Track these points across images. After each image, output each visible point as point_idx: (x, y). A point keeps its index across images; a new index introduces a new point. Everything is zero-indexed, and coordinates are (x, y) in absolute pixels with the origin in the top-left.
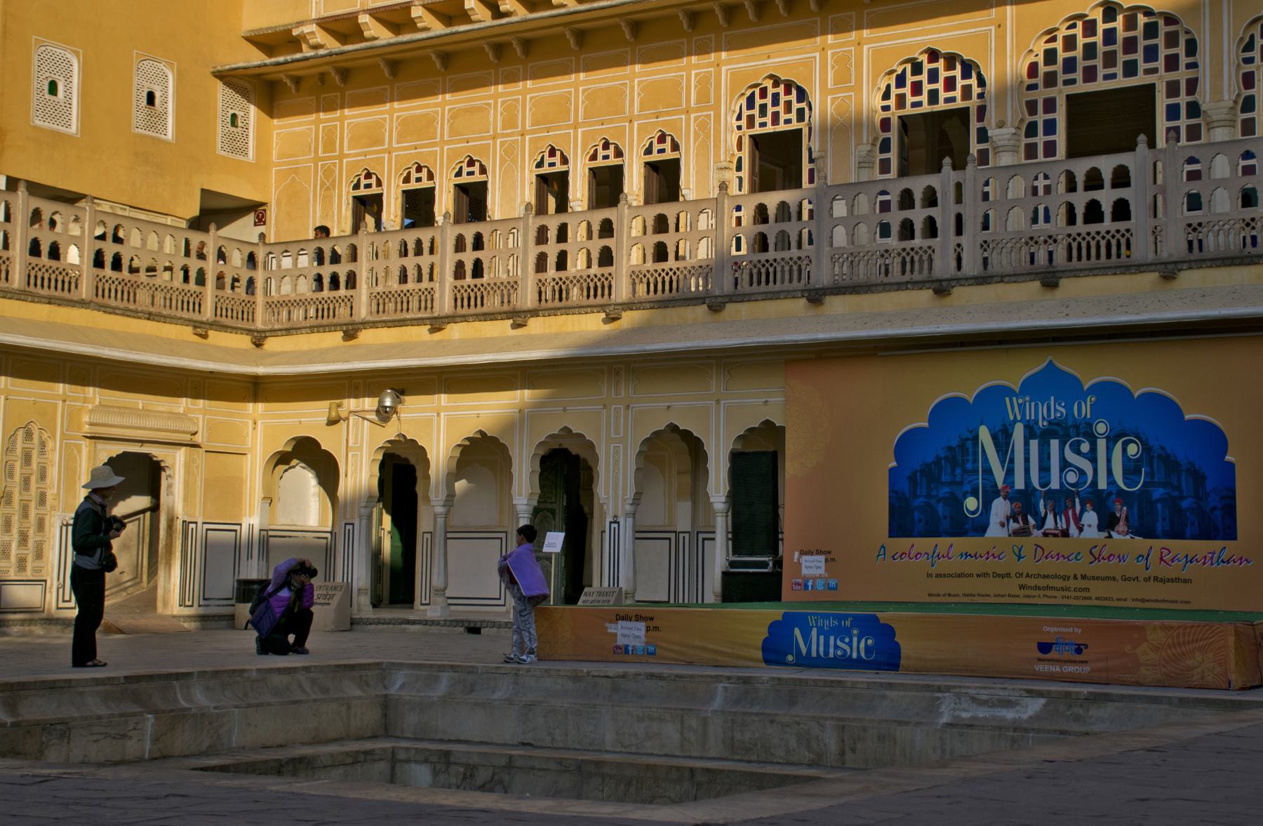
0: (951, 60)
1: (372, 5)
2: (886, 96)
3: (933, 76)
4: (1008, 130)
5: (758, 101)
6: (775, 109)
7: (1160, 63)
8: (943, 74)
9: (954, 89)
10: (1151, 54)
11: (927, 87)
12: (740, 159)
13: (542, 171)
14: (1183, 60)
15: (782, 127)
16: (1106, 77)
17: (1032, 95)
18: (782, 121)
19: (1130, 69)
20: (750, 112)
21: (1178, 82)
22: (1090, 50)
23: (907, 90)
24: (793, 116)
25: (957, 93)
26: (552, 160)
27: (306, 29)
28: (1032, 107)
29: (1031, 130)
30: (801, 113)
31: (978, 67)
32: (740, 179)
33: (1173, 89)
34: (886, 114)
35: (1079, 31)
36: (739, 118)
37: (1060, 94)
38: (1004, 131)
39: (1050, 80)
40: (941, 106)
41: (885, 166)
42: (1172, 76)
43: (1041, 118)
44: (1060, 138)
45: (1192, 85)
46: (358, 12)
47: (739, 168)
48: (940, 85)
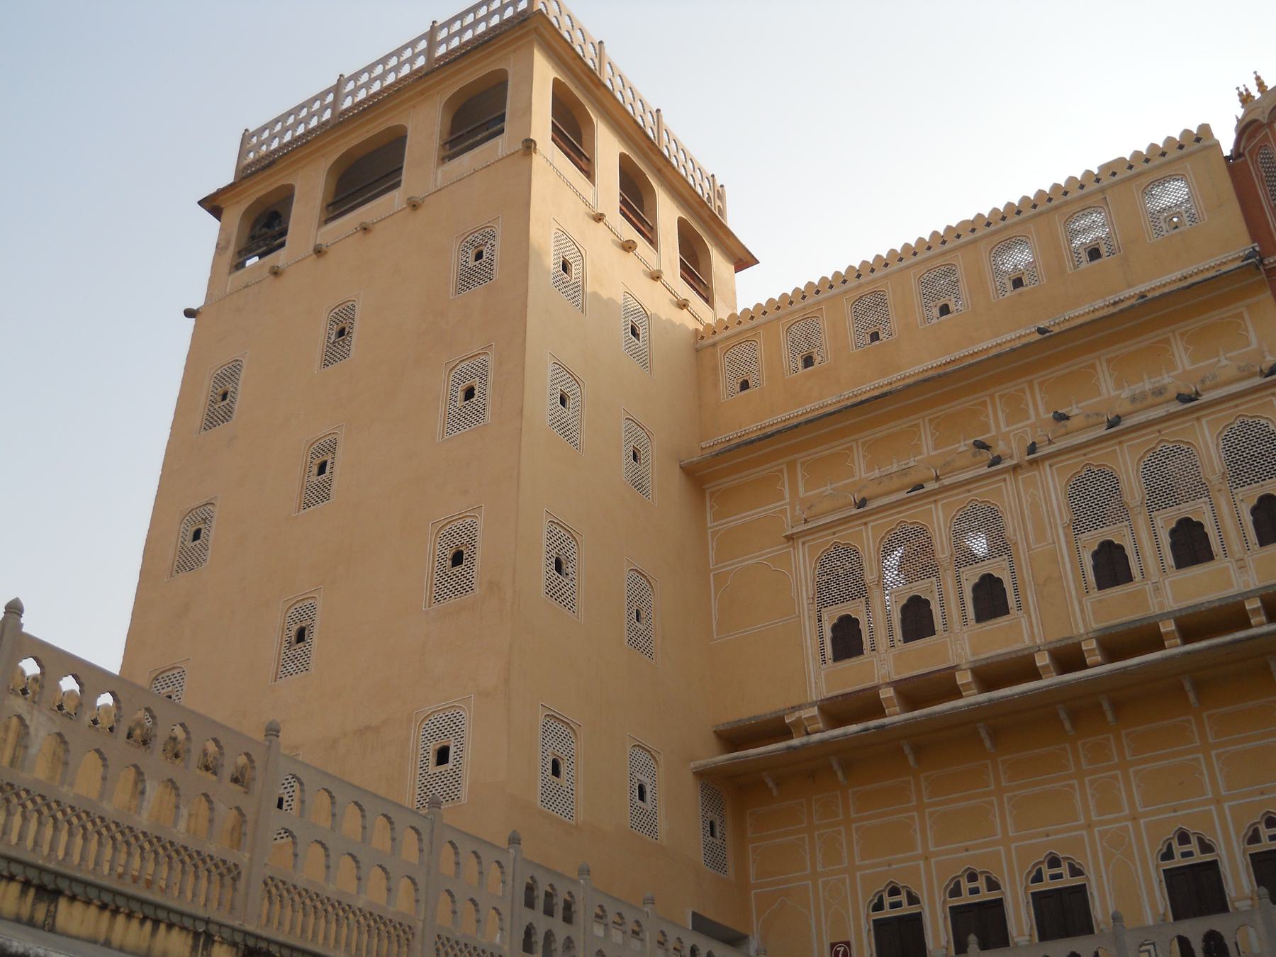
1: (896, 677)
13: (1169, 864)
26: (1186, 848)
46: (876, 689)
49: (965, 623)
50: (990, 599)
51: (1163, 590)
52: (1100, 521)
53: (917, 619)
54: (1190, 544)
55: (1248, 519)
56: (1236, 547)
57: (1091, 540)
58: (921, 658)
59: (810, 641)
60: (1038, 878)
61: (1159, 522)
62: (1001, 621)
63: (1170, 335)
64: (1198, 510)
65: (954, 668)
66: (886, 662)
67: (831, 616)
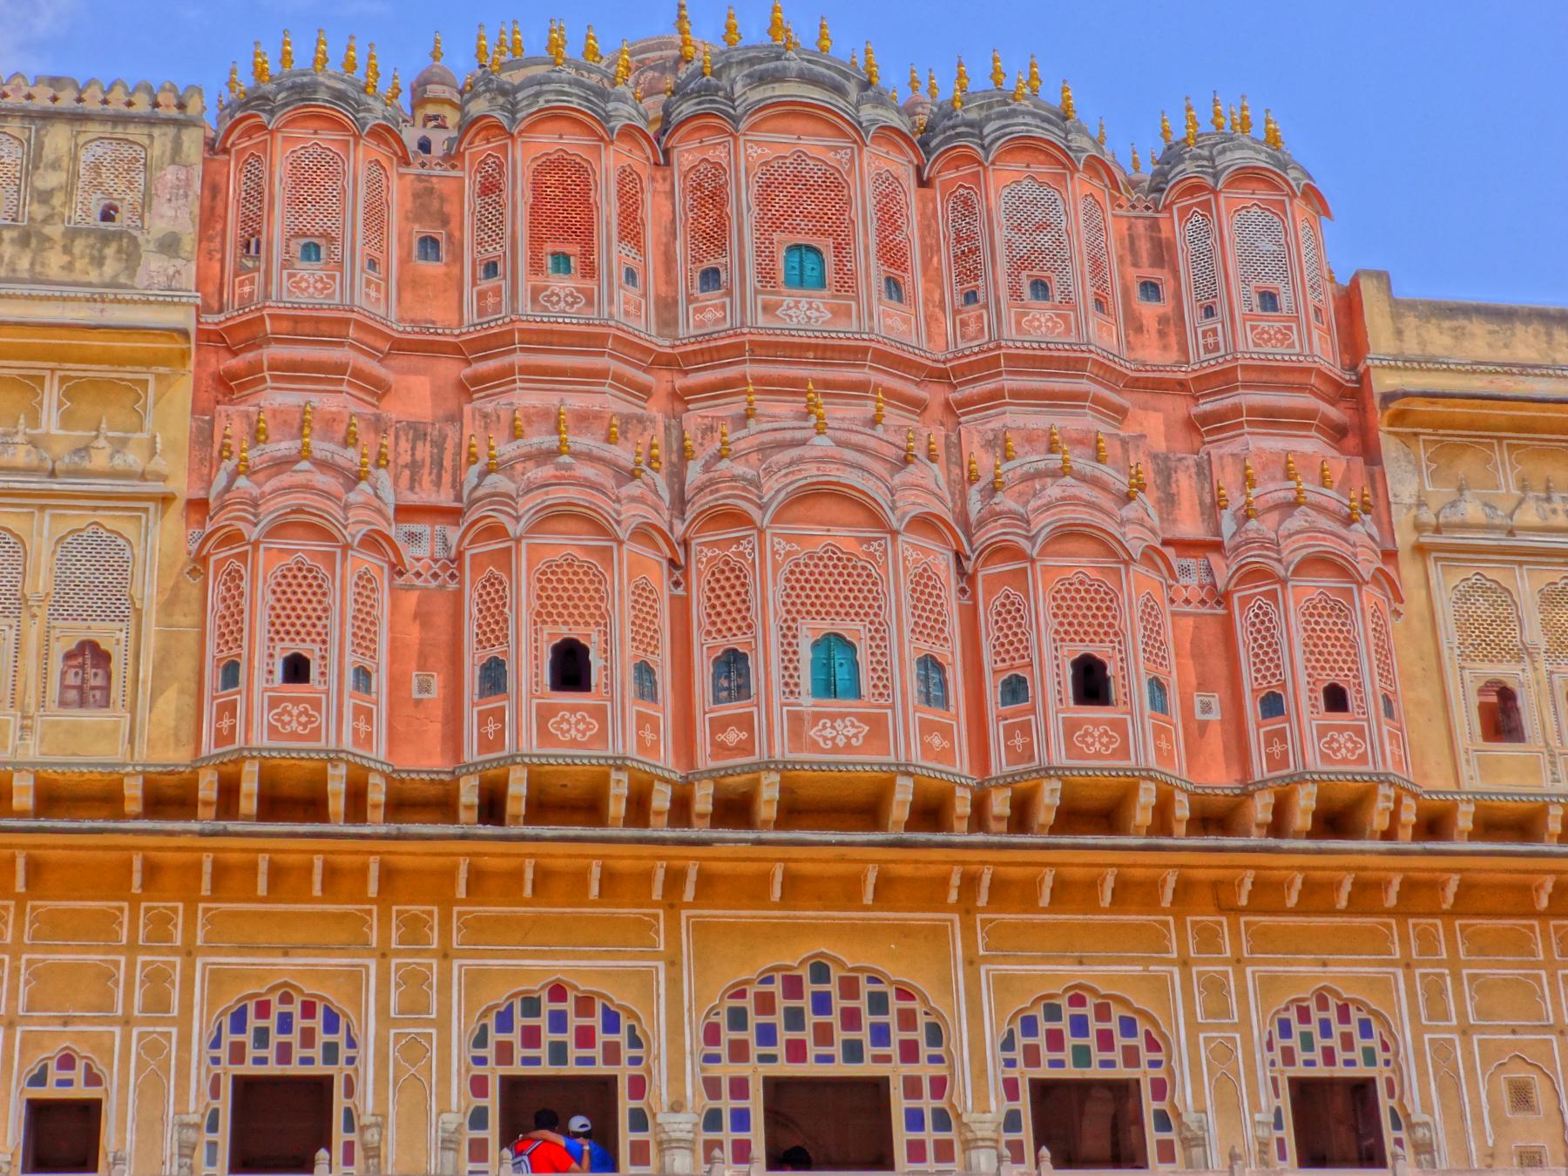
0: (585, 1004)
2: (481, 1041)
3: (558, 1022)
5: (253, 1022)
6: (284, 1038)
7: (894, 1050)
8: (573, 1022)
9: (591, 1045)
10: (881, 1035)
11: (547, 1037)
12: (215, 1114)
14: (925, 1051)
15: (294, 1069)
16: (821, 1059)
17: (714, 1070)
18: (295, 1058)
19: (853, 1052)
20: (238, 1038)
21: (918, 1079)
22: (795, 1019)
23: (515, 1037)
24: (317, 1052)
25: (597, 1052)
28: (712, 1087)
29: (713, 1120)
30: (331, 1052)
31: (632, 1014)
32: (212, 1146)
33: (912, 1087)
34: (479, 1070)
35: (777, 988)
36: (216, 1044)
37: (755, 1073)
38: (680, 1117)
39: (739, 1052)
40: (571, 1069)
43: (727, 1104)
44: (757, 1136)
45: (939, 1086)
47: (213, 1126)
48: (569, 1037)
55: (56, 664)
56: (31, 699)
63: (47, 374)
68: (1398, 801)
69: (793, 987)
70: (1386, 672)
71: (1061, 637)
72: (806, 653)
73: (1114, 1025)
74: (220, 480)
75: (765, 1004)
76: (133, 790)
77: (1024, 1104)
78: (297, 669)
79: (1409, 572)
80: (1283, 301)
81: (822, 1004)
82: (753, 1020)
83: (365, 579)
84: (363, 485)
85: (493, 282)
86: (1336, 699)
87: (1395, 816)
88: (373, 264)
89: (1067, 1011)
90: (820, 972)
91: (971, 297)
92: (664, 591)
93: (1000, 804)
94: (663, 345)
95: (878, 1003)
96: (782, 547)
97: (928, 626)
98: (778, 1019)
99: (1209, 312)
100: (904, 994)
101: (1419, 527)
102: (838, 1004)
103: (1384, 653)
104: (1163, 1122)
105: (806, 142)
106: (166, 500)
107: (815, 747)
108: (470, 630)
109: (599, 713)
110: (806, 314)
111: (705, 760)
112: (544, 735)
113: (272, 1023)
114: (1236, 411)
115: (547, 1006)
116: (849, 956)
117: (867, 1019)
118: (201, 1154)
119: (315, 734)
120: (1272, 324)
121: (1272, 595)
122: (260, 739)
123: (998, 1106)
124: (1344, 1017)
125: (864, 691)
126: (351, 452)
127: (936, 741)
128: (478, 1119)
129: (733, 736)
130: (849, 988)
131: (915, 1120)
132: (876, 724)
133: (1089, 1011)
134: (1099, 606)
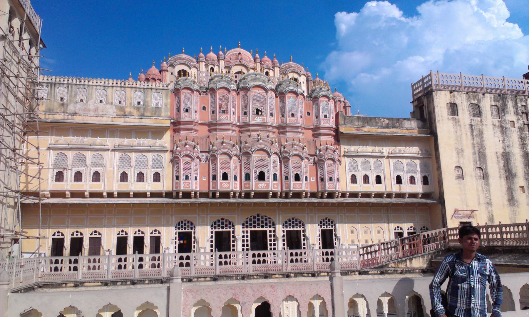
0: (226, 221)
4: (241, 236)
5: (181, 224)
8: (225, 223)
10: (266, 224)
22: (255, 222)
27: (46, 193)
29: (243, 237)
33: (270, 231)
35: (252, 218)
39: (247, 227)
41: (212, 241)
42: (270, 229)
43: (245, 234)
45: (274, 231)
47: (176, 239)
49: (90, 181)
50: (97, 177)
51: (133, 186)
52: (124, 167)
53: (78, 177)
54: (141, 177)
55: (152, 176)
56: (149, 181)
57: (121, 170)
58: (77, 187)
59: (50, 175)
60: (91, 234)
61: (136, 171)
62: (98, 183)
64: (144, 171)
65: (85, 191)
66: (68, 185)
67: (56, 171)
68: (338, 194)
69: (254, 218)
70: (338, 174)
71: (293, 171)
72: (258, 174)
73: (298, 222)
74: (175, 148)
75: (251, 220)
76: (164, 194)
77: (285, 234)
78: (187, 178)
79: (343, 159)
80: (328, 116)
81: (258, 220)
82: (249, 222)
83: (196, 163)
84: (196, 149)
85: (214, 114)
86: (331, 179)
87: (338, 196)
88: (196, 112)
89: (292, 220)
90: (258, 215)
91: (283, 116)
92: (238, 163)
93: (284, 195)
94: (238, 124)
95: (266, 220)
96: (255, 158)
97: (275, 168)
98: (252, 222)
99: (317, 118)
100: (269, 218)
101: (344, 152)
102: (261, 220)
103: (338, 171)
104: (304, 236)
105: (260, 91)
106: (167, 151)
107: (259, 188)
108: (211, 170)
109: (229, 183)
110: (258, 120)
111: (243, 189)
112: (221, 187)
113: (183, 224)
114: (320, 134)
115: (221, 221)
116: (262, 214)
117: (264, 222)
118: (174, 243)
119: (190, 187)
120: (325, 120)
121: (323, 164)
122: (182, 188)
123: (282, 234)
124: (329, 221)
125: (266, 179)
126: (193, 143)
127: (275, 186)
128: (212, 237)
129: (247, 186)
130: (262, 218)
131: (270, 236)
132: (267, 184)
133: (294, 220)
134: (299, 166)
